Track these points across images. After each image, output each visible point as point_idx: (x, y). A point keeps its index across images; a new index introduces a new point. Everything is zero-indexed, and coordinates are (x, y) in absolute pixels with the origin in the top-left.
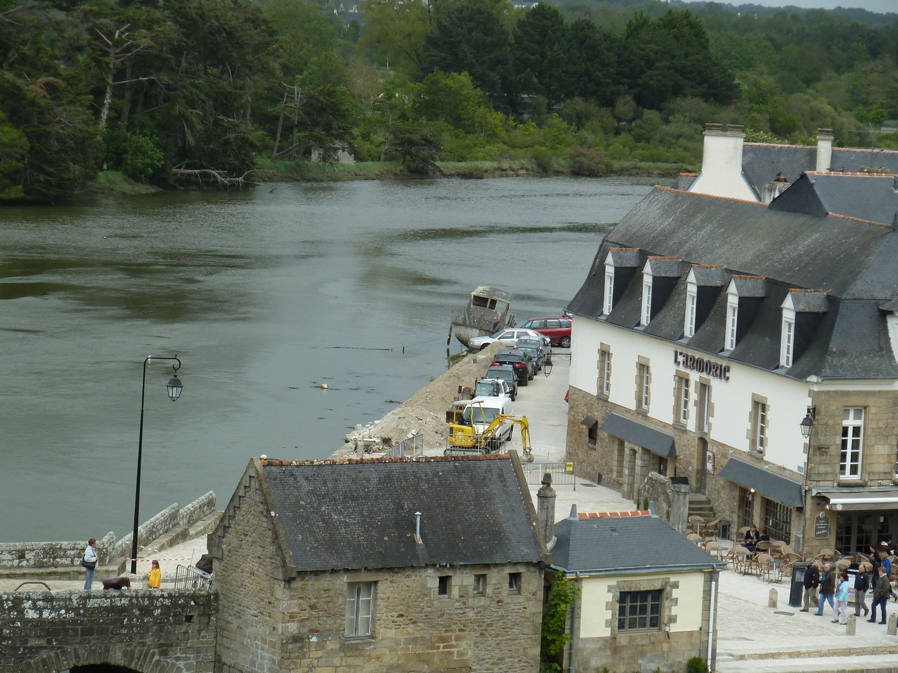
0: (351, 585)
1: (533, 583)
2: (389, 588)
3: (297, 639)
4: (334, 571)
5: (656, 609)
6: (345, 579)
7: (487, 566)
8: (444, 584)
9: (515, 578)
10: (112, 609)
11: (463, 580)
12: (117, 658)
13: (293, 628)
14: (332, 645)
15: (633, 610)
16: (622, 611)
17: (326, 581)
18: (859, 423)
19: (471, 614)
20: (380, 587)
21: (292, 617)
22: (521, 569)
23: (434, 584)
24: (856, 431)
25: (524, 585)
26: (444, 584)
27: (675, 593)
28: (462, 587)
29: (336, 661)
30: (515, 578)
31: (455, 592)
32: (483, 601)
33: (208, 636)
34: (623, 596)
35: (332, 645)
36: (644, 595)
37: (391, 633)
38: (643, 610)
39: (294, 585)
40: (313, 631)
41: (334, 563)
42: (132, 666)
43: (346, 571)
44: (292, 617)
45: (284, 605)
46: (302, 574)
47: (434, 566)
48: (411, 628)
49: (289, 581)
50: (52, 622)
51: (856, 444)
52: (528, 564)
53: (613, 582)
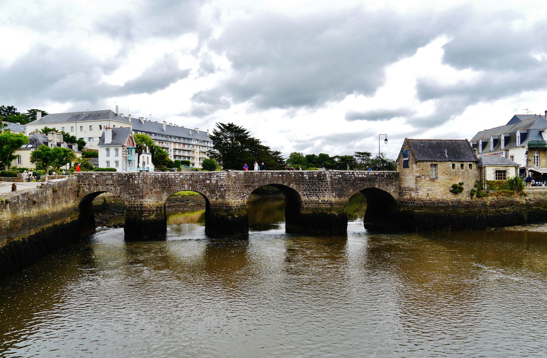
0: (431, 165)
1: (474, 166)
2: (440, 166)
3: (419, 177)
4: (427, 161)
5: (504, 175)
6: (430, 163)
7: (463, 162)
8: (453, 165)
9: (470, 165)
10: (375, 175)
11: (458, 165)
12: (377, 187)
13: (418, 174)
14: (428, 179)
15: (499, 175)
16: (496, 175)
17: (425, 163)
18: (538, 155)
19: (460, 173)
20: (438, 166)
21: (417, 172)
22: (471, 163)
23: (451, 165)
24: (537, 157)
25: (473, 167)
26: (453, 166)
27: (509, 171)
28: (458, 167)
29: (429, 183)
30: (470, 165)
31: (456, 168)
32: (463, 170)
33: (397, 183)
34: (496, 172)
35: (428, 179)
36: (501, 171)
37: (442, 177)
38: (501, 175)
39: (418, 164)
40: (423, 175)
41: (427, 159)
42: (381, 188)
43: (430, 161)
44: (417, 172)
45: (415, 169)
46: (419, 161)
47: (451, 161)
48: (446, 176)
49: (416, 163)
50: (361, 178)
51: (537, 160)
52: (473, 162)
53: (494, 168)
